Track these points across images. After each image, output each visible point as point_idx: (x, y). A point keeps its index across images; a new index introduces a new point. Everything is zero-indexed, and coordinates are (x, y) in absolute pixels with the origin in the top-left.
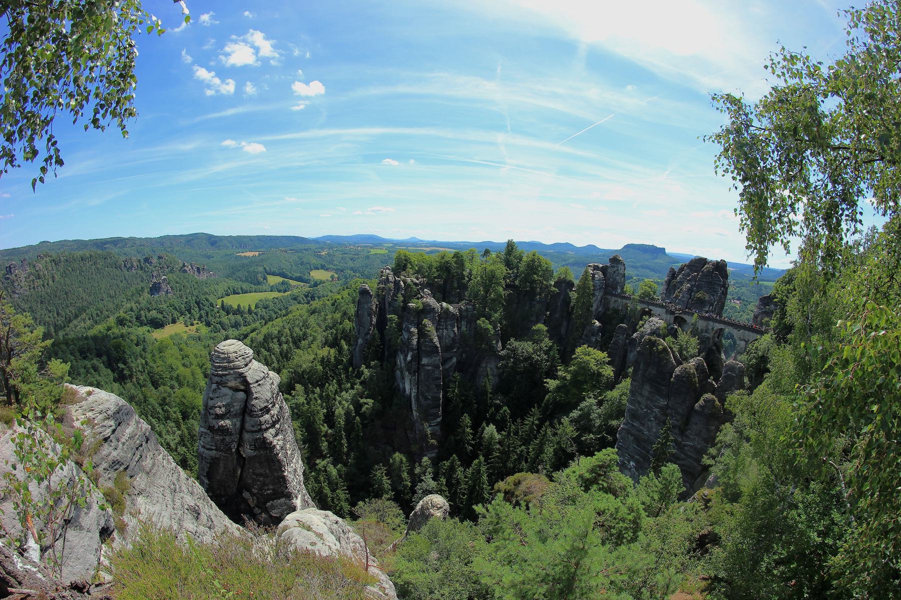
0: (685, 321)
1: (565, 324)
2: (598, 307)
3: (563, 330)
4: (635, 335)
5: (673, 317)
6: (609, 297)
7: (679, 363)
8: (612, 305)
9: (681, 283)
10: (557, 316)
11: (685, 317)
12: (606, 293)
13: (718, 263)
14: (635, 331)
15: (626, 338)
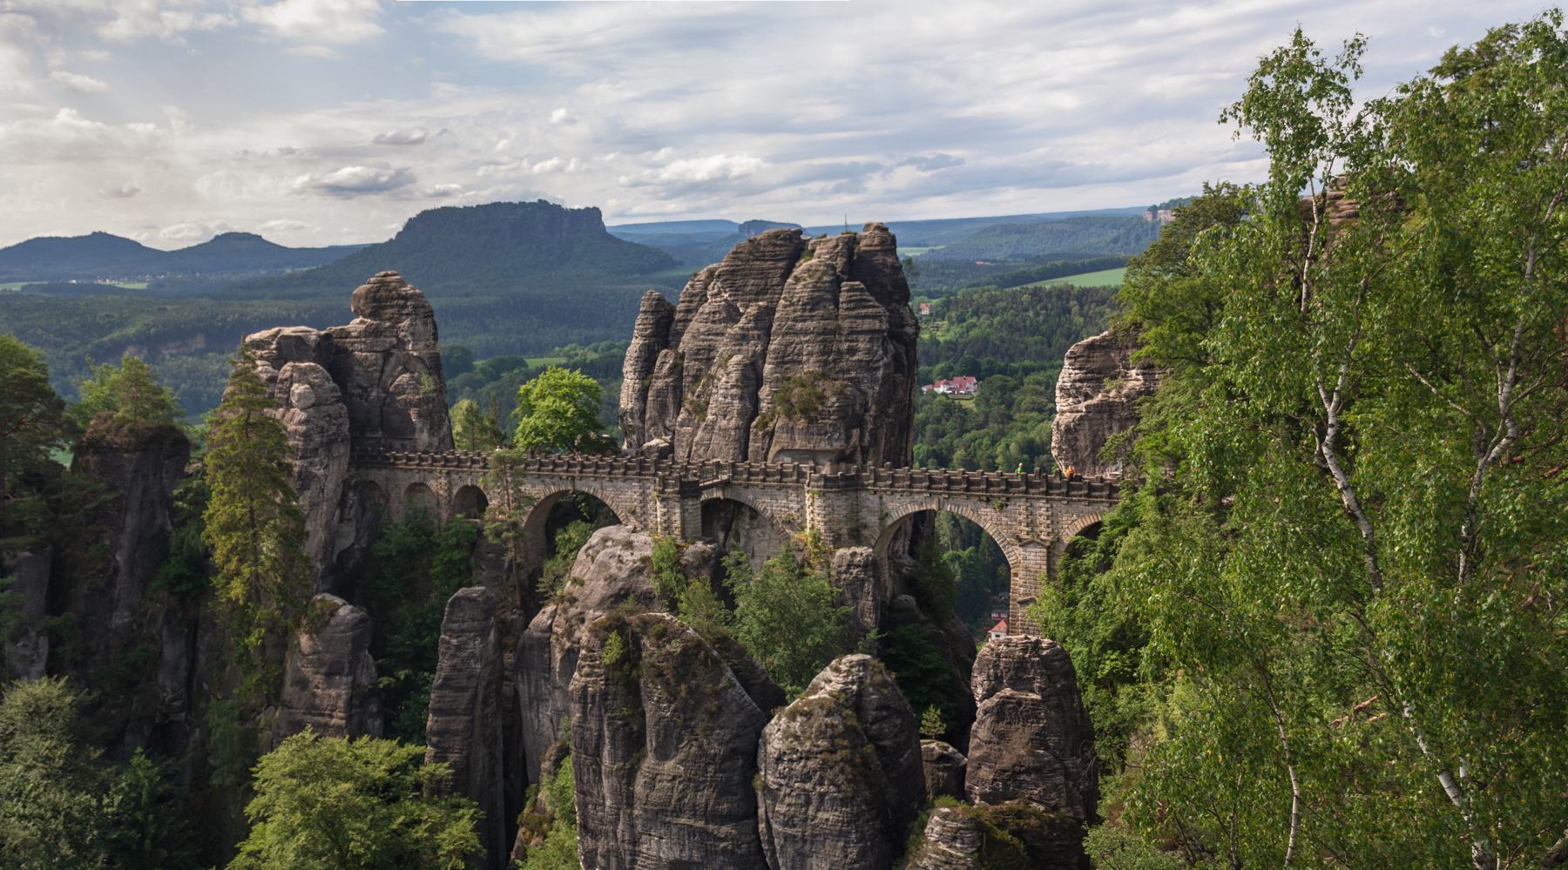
0: (755, 514)
1: (171, 651)
2: (333, 536)
3: (167, 685)
4: (542, 619)
5: (693, 505)
6: (378, 475)
7: (772, 700)
8: (398, 511)
9: (706, 355)
10: (120, 619)
11: (748, 496)
12: (361, 459)
13: (851, 241)
14: (532, 603)
15: (501, 647)
